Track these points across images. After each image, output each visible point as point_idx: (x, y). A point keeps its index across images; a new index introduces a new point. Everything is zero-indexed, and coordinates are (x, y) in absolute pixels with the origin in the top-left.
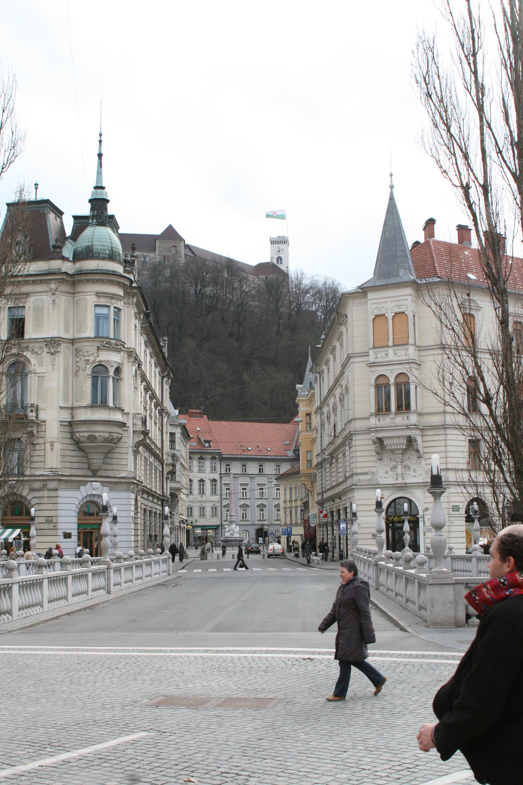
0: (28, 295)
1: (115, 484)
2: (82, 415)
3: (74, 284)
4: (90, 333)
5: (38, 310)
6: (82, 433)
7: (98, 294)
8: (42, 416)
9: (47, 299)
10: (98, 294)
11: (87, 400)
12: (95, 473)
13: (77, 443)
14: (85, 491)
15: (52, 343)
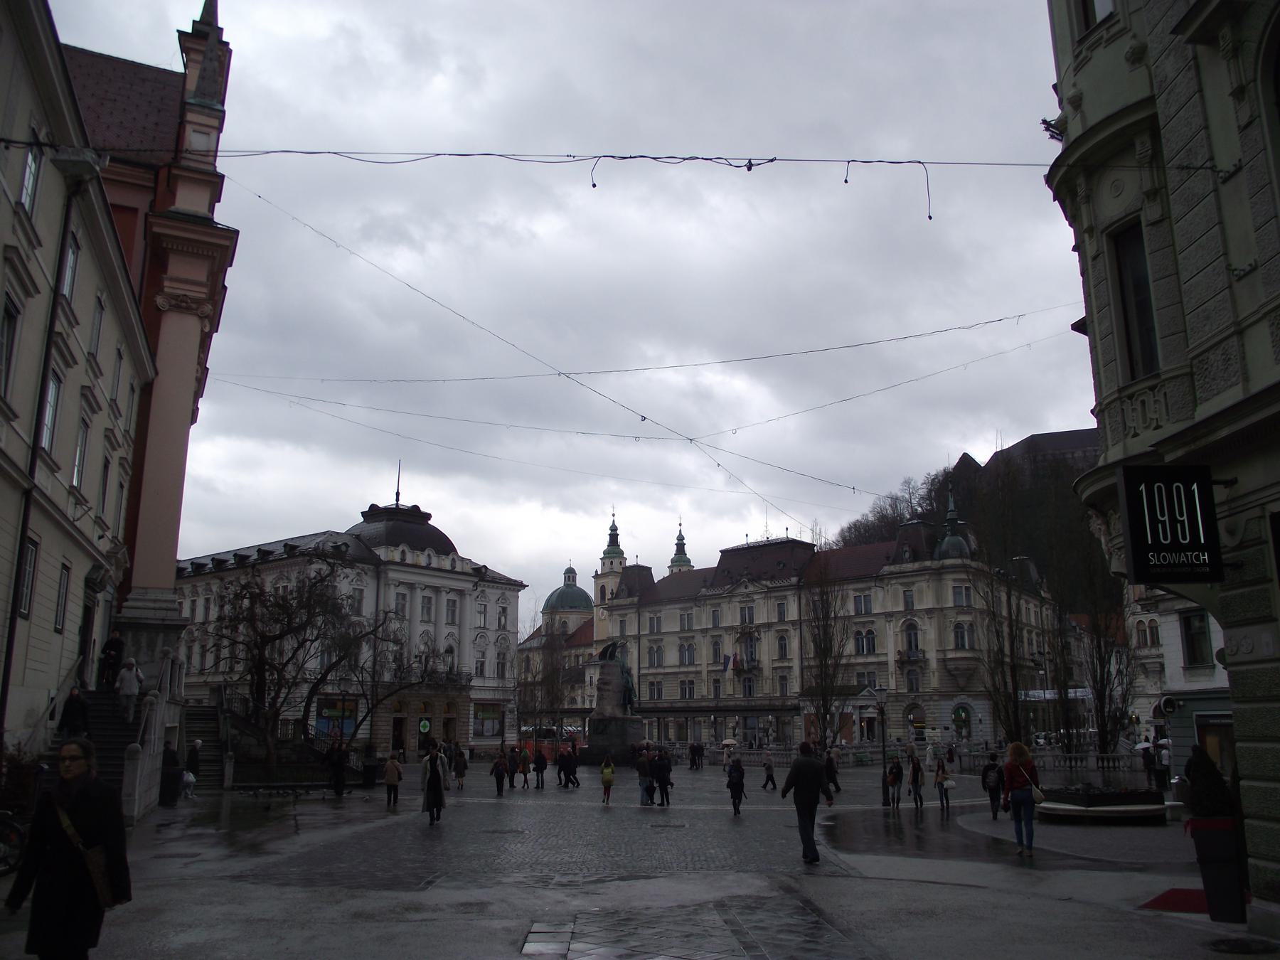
0: (913, 583)
1: (976, 696)
2: (950, 655)
3: (940, 574)
4: (951, 604)
5: (920, 592)
6: (951, 666)
7: (955, 580)
8: (928, 656)
9: (924, 585)
10: (955, 580)
11: (952, 646)
12: (962, 690)
13: (949, 671)
14: (956, 701)
15: (929, 611)
